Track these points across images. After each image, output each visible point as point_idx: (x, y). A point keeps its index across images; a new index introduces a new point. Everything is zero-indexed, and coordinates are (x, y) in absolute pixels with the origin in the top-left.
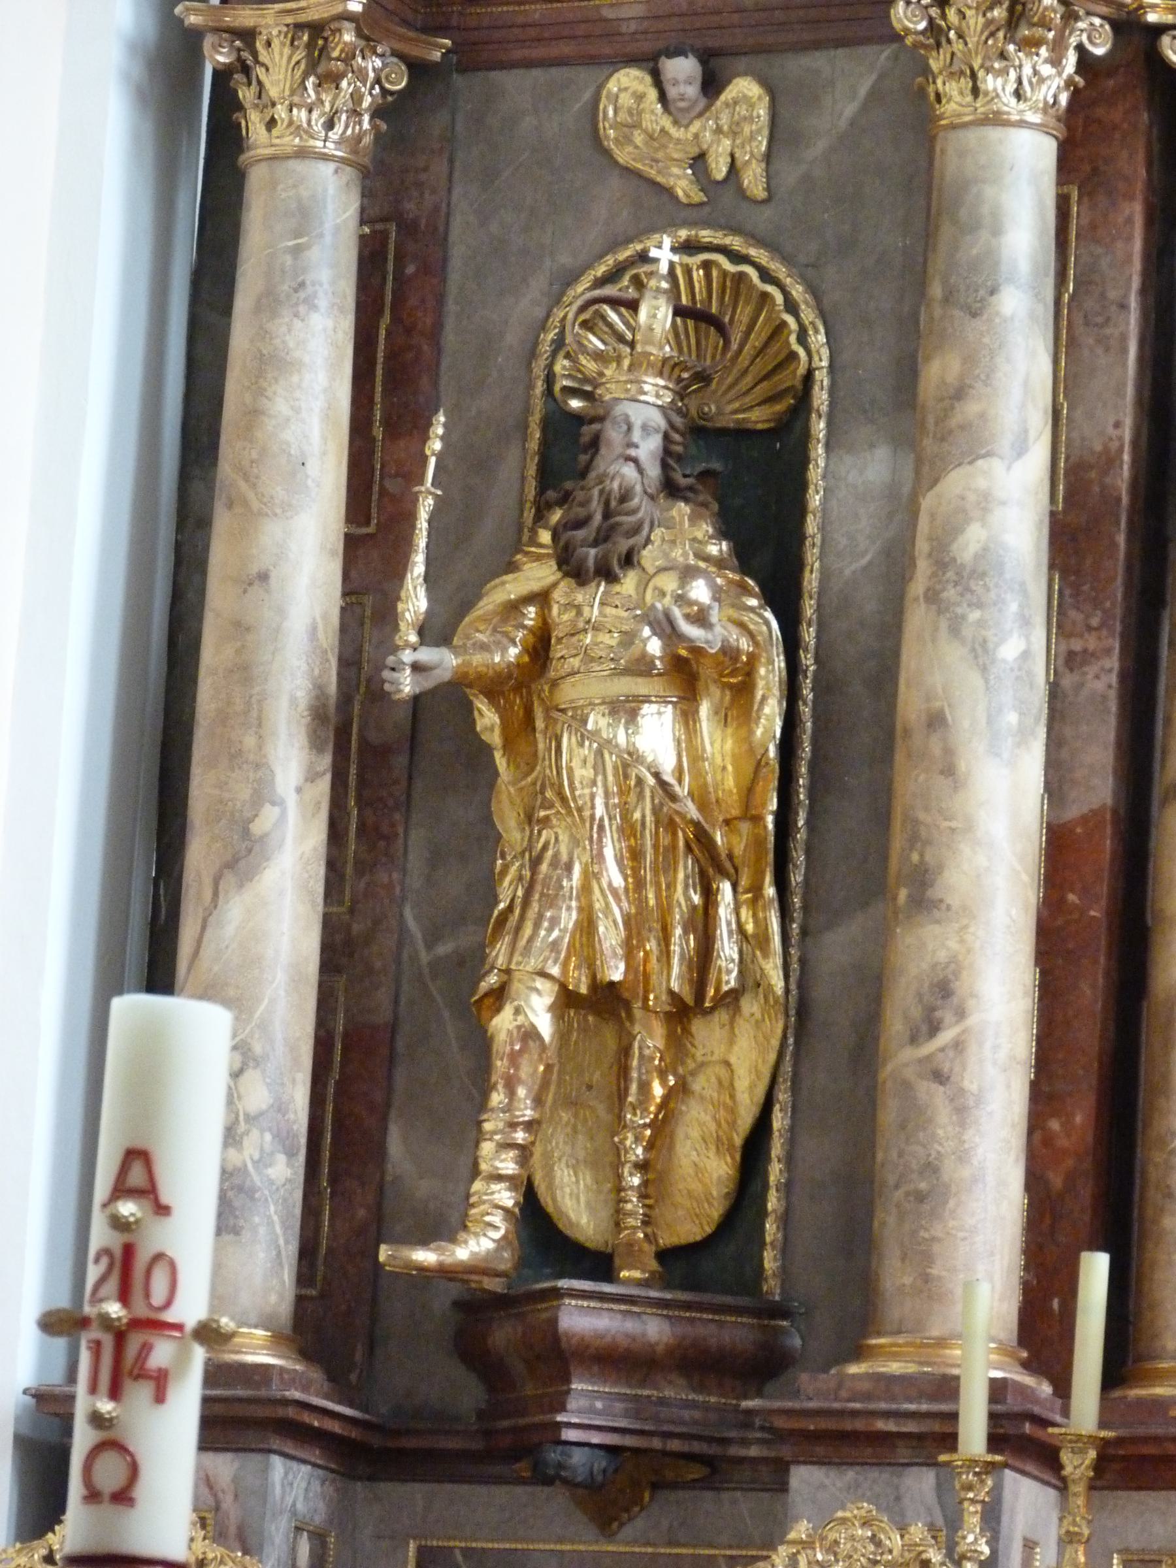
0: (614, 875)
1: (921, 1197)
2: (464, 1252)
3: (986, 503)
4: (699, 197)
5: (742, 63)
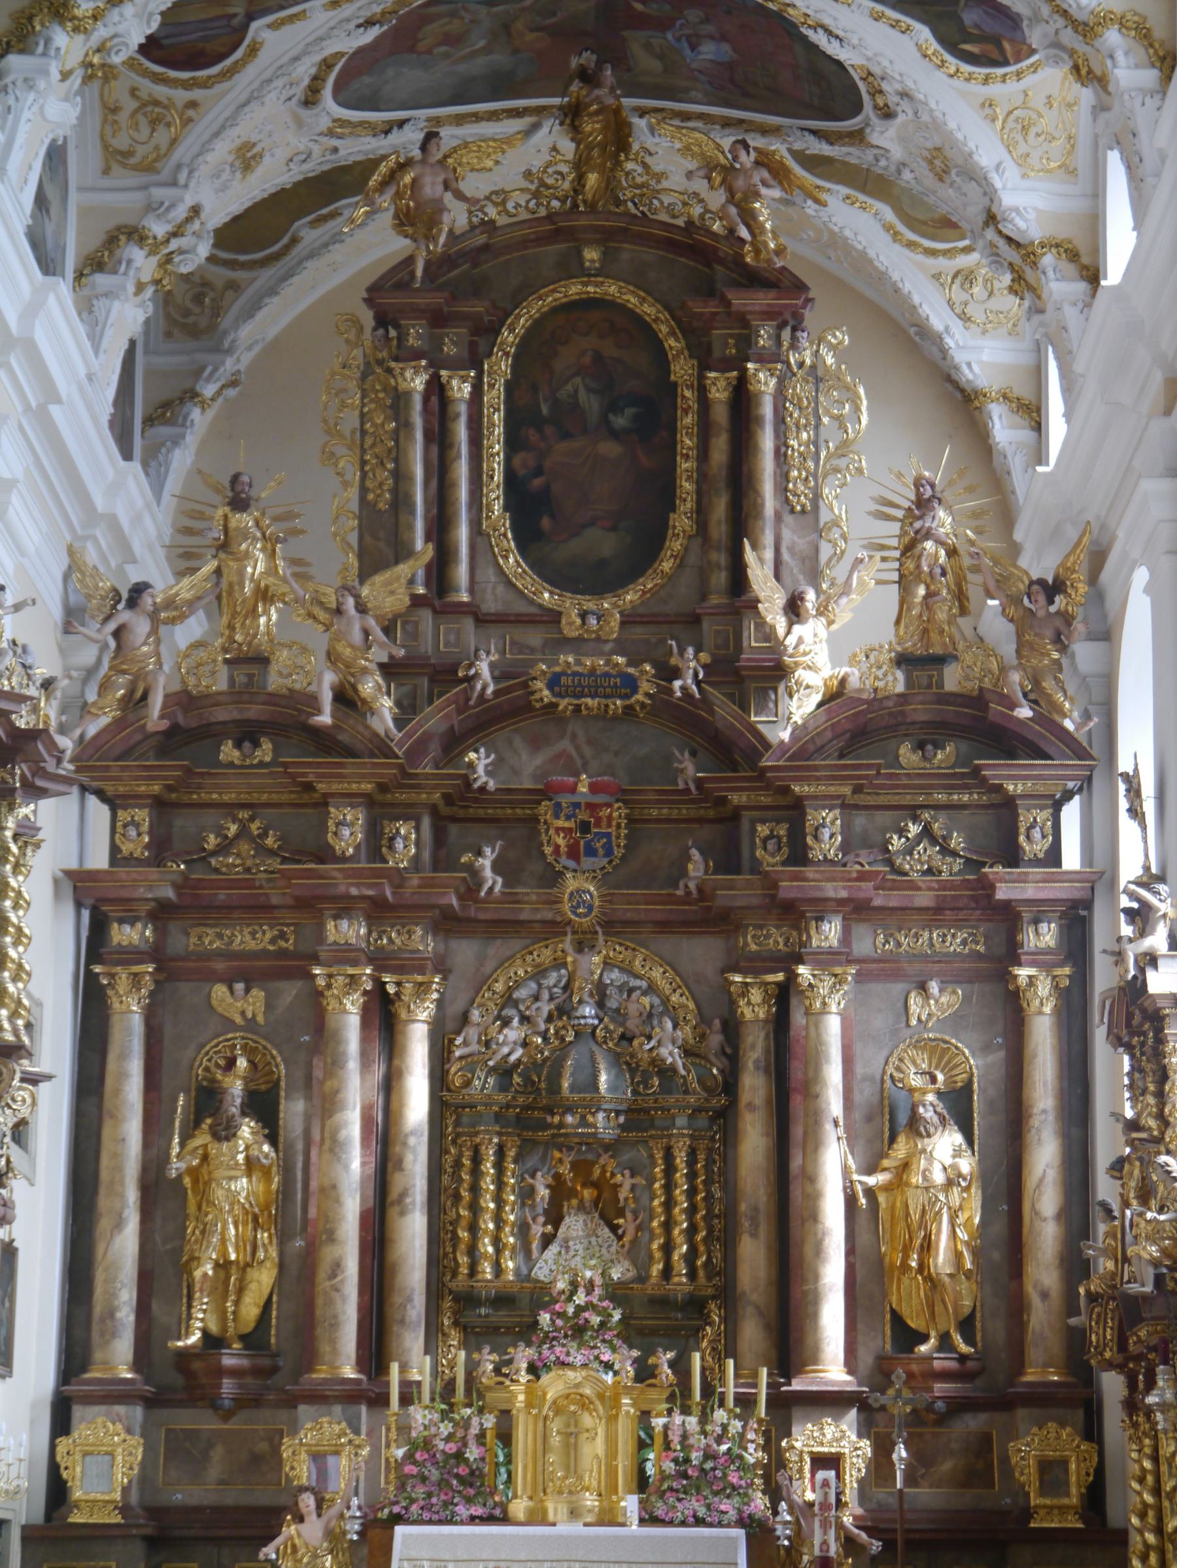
1: (331, 1325)
3: (345, 1124)
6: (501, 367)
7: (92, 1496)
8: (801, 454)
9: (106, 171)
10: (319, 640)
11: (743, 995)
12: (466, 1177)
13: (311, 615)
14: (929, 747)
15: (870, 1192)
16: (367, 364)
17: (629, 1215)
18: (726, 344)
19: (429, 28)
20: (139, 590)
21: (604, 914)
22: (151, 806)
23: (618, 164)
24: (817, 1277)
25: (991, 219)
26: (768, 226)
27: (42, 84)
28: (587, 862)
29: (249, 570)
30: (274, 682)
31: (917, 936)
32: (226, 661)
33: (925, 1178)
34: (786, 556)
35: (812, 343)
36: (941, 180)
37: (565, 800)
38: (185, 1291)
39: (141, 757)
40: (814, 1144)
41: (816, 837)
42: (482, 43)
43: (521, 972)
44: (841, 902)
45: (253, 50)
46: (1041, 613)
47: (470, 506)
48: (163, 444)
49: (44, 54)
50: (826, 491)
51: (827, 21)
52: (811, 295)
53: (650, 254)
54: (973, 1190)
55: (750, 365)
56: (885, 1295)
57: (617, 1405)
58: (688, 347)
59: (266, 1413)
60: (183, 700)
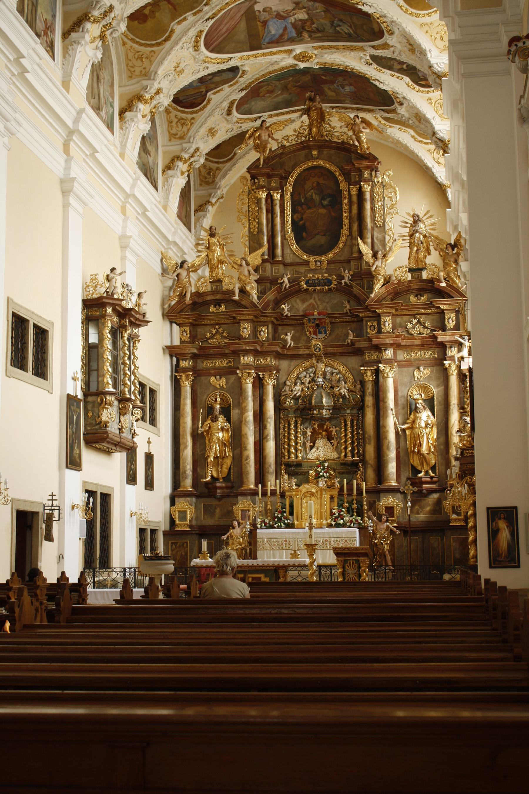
0: (218, 448)
2: (207, 479)
3: (249, 416)
6: (289, 188)
7: (181, 523)
8: (379, 209)
9: (170, 140)
10: (236, 274)
13: (233, 267)
14: (419, 296)
15: (404, 430)
16: (249, 191)
17: (335, 439)
18: (355, 177)
19: (262, 89)
20: (183, 263)
22: (190, 326)
23: (322, 125)
24: (387, 456)
25: (434, 133)
26: (364, 141)
27: (136, 120)
28: (320, 336)
29: (216, 255)
30: (225, 288)
31: (417, 353)
32: (210, 282)
33: (419, 425)
34: (375, 240)
35: (381, 175)
36: (420, 122)
37: (311, 317)
39: (186, 312)
40: (386, 416)
41: (384, 325)
42: (279, 92)
43: (301, 370)
44: (392, 345)
45: (209, 101)
46: (450, 254)
47: (281, 231)
48: (201, 217)
49: (136, 111)
50: (387, 220)
51: (378, 78)
52: (379, 161)
53: (332, 152)
54: (434, 428)
55: (362, 183)
56: (409, 460)
57: (321, 495)
58: (345, 179)
60: (197, 294)
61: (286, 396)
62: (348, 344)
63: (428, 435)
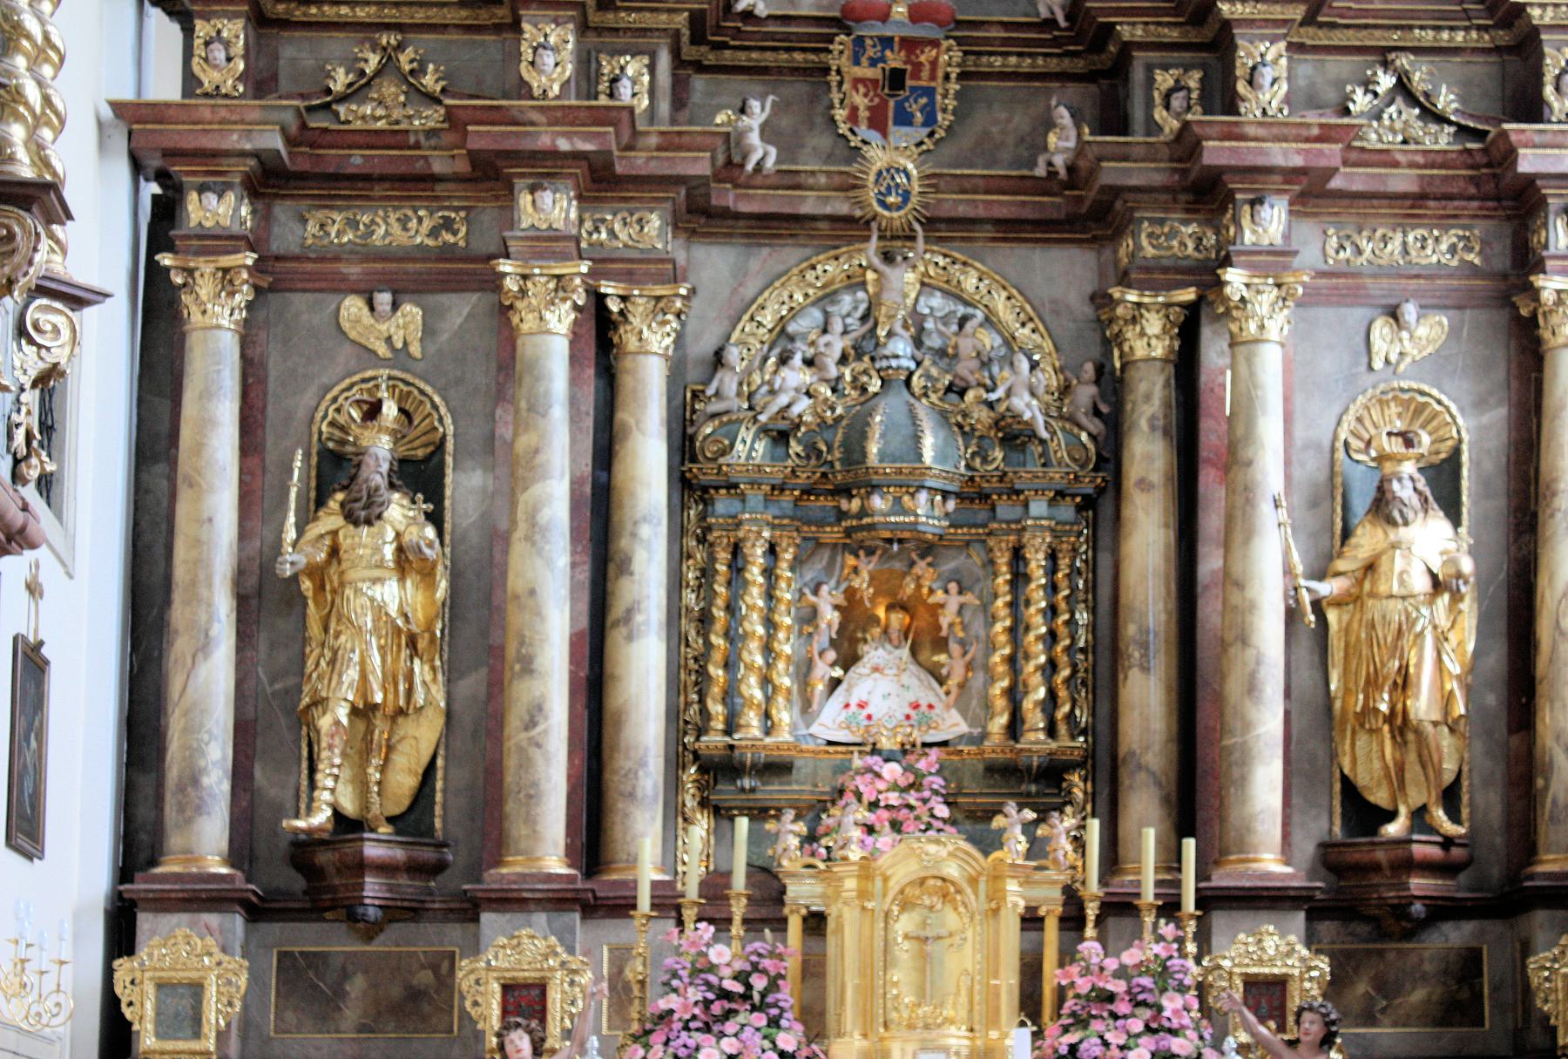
1: (530, 797)
4: (389, 355)
5: (407, 297)
7: (170, 1045)
11: (1134, 320)
12: (721, 589)
21: (926, 206)
31: (1385, 240)
38: (305, 753)
44: (1292, 174)
59: (429, 929)
61: (728, 423)
62: (1052, 174)
63: (1441, 638)
